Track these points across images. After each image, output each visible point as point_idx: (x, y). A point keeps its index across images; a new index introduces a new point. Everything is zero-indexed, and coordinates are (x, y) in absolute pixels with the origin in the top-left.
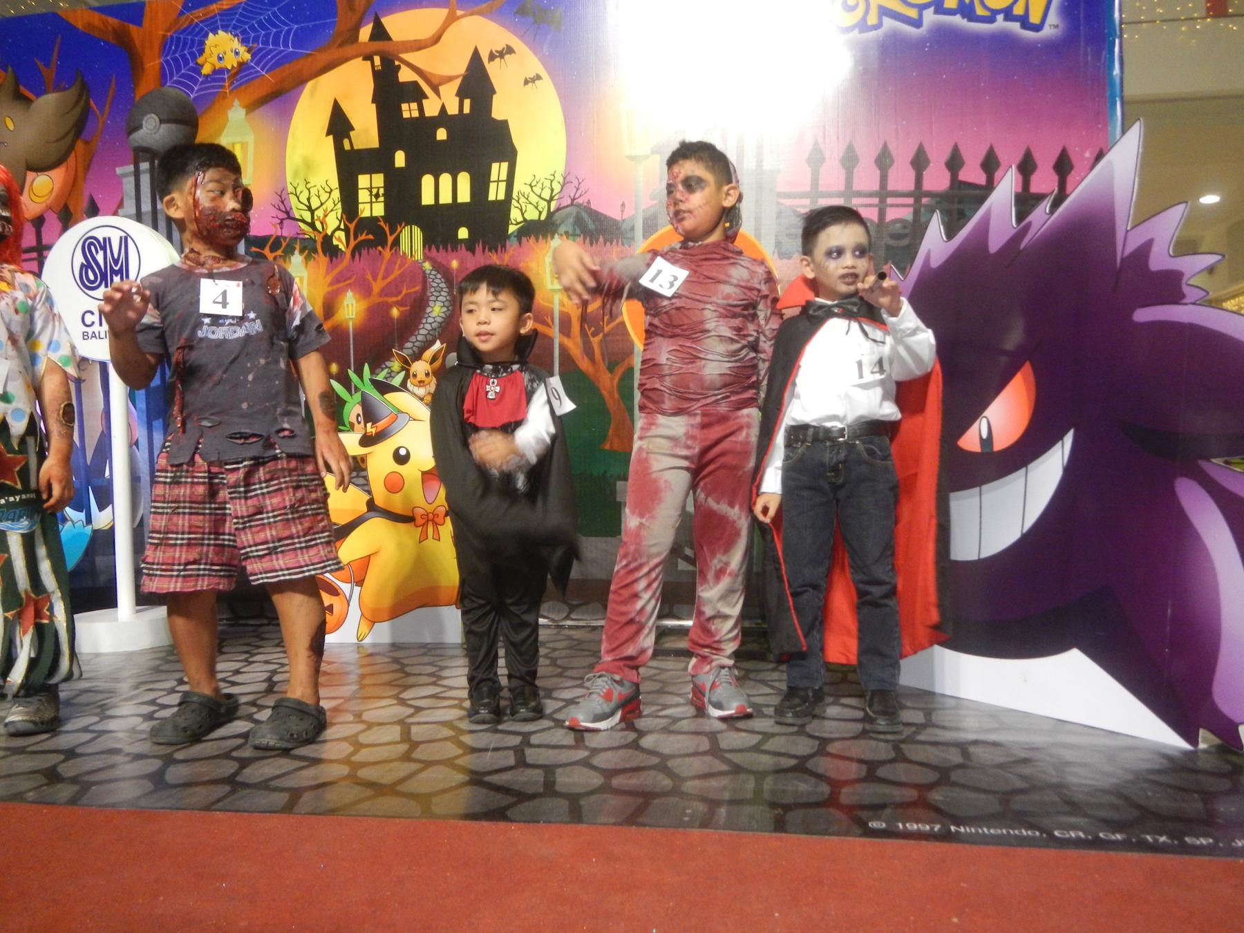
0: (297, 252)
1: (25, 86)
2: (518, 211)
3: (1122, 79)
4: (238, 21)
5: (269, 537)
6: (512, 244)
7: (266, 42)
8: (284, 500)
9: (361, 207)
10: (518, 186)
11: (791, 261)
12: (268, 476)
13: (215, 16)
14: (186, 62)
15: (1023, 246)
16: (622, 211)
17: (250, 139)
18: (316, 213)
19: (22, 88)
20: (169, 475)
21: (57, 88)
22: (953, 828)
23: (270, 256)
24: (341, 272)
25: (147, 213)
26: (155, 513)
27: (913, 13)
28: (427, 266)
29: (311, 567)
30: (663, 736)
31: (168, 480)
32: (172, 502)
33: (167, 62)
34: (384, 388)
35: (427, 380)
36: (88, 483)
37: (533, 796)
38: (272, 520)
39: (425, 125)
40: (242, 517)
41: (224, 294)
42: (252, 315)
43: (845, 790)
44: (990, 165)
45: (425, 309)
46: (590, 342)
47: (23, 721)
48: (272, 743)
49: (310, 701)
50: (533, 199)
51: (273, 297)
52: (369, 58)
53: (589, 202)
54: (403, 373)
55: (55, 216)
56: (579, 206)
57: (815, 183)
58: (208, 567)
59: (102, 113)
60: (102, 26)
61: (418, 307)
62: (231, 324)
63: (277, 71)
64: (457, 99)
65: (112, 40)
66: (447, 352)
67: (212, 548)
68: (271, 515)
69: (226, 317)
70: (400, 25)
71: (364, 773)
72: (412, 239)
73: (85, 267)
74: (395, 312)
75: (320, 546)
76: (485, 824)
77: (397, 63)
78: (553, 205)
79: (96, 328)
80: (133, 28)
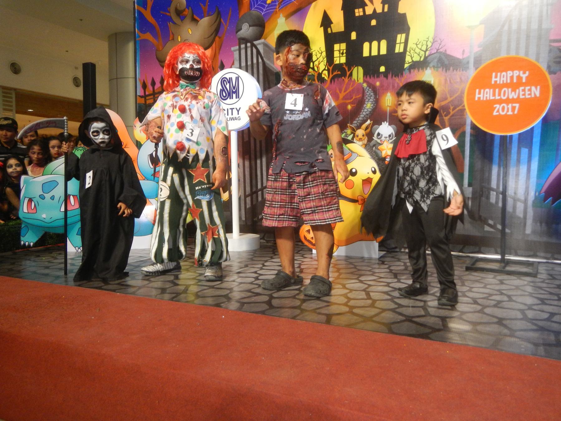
1: (195, 15)
2: (410, 58)
5: (312, 206)
6: (406, 73)
8: (319, 190)
9: (335, 59)
10: (410, 45)
11: (557, 75)
12: (312, 179)
16: (463, 54)
18: (315, 63)
19: (195, 17)
20: (273, 177)
21: (208, 15)
26: (268, 193)
28: (365, 85)
29: (329, 220)
30: (496, 310)
31: (273, 179)
32: (274, 189)
34: (346, 141)
35: (363, 138)
37: (439, 330)
38: (314, 198)
39: (366, 18)
40: (302, 197)
41: (296, 100)
42: (307, 109)
45: (363, 105)
46: (443, 119)
47: (211, 275)
48: (313, 294)
49: (326, 278)
50: (418, 51)
51: (316, 100)
53: (446, 51)
54: (352, 135)
58: (288, 217)
59: (226, 24)
61: (360, 104)
62: (298, 114)
64: (382, 5)
66: (373, 125)
67: (289, 209)
68: (313, 196)
69: (296, 111)
71: (355, 311)
72: (358, 73)
73: (222, 91)
74: (349, 107)
75: (334, 211)
76: (421, 340)
78: (427, 53)
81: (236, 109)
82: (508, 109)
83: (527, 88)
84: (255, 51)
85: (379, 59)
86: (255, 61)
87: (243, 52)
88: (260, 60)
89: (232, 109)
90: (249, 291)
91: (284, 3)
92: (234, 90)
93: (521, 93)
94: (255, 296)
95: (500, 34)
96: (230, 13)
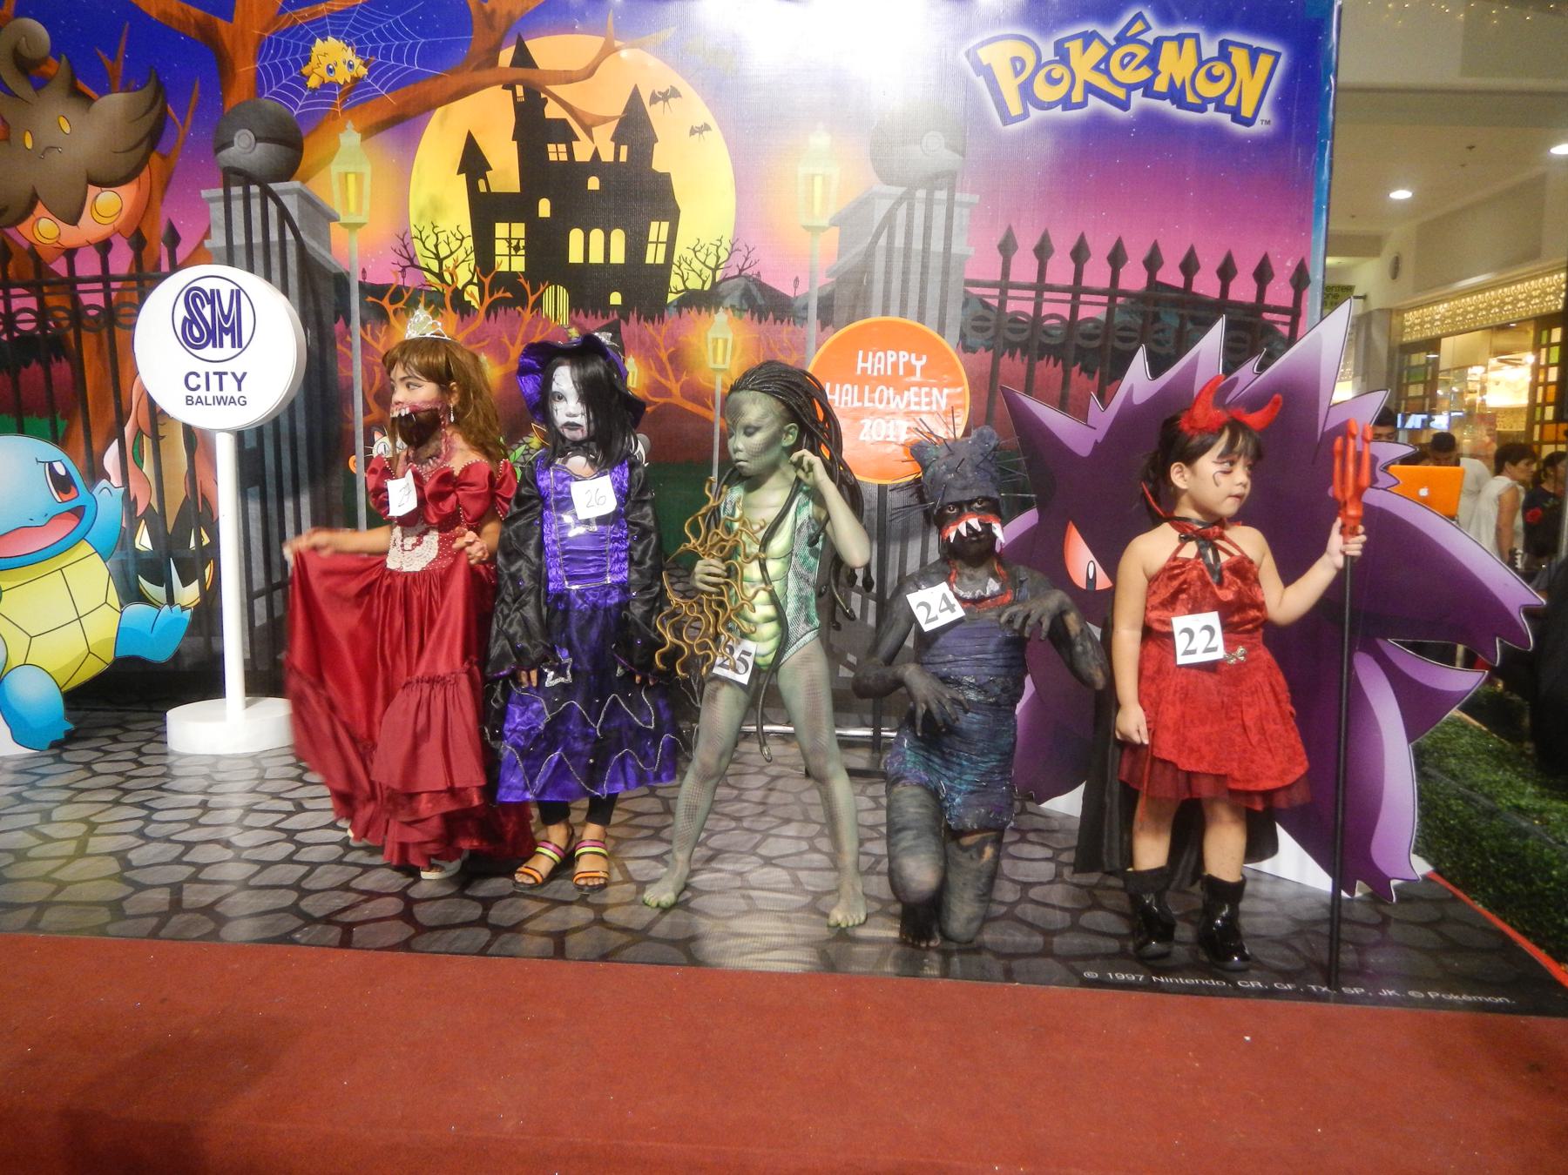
0: (421, 306)
3: (1329, 186)
4: (352, 27)
6: (670, 315)
7: (386, 56)
10: (680, 250)
11: (974, 356)
13: (324, 18)
14: (288, 72)
15: (1228, 400)
17: (367, 169)
18: (445, 262)
19: (81, 85)
21: (125, 88)
22: (1154, 978)
23: (390, 309)
24: (473, 333)
25: (240, 247)
27: (1120, 93)
33: (264, 68)
36: (170, 555)
39: (574, 172)
43: (1056, 940)
44: (1189, 266)
50: (697, 265)
52: (510, 86)
53: (759, 274)
55: (125, 241)
56: (747, 277)
57: (1006, 272)
59: (183, 126)
60: (182, 17)
63: (400, 91)
64: (613, 144)
65: (193, 33)
70: (549, 51)
72: (556, 301)
73: (189, 322)
77: (543, 96)
78: (718, 278)
79: (202, 392)
80: (221, 23)
81: (234, 374)
82: (888, 428)
83: (925, 390)
84: (272, 208)
85: (605, 276)
86: (274, 236)
87: (237, 207)
88: (290, 236)
89: (221, 374)
90: (345, 887)
91: (356, 96)
92: (226, 323)
93: (914, 399)
94: (366, 901)
95: (869, 254)
96: (196, 94)
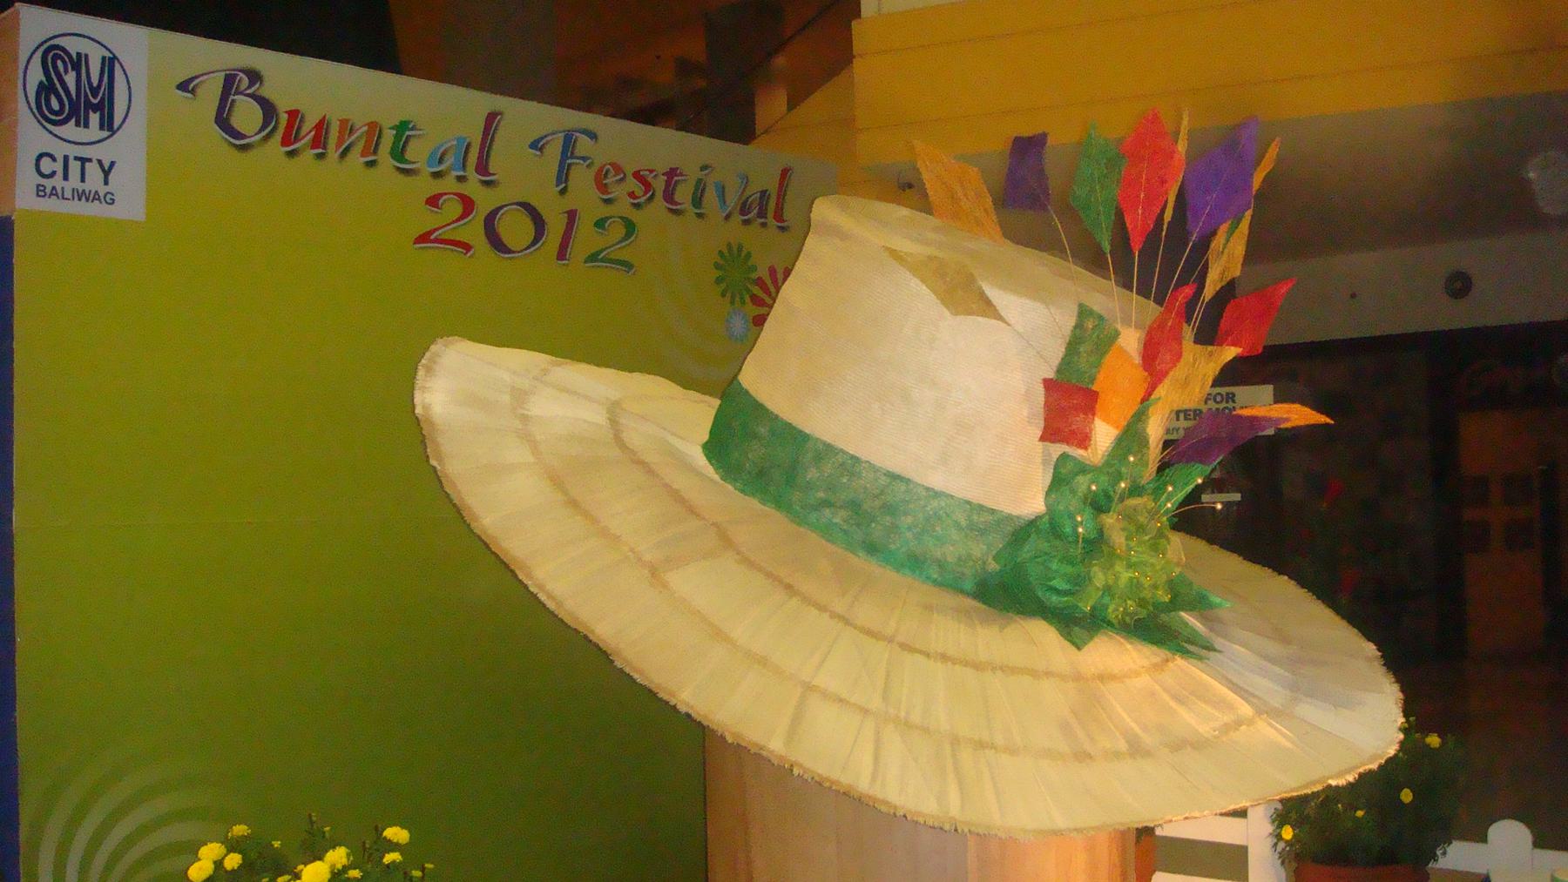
73: (45, 90)
79: (57, 181)
81: (100, 162)
89: (83, 161)
92: (95, 96)
